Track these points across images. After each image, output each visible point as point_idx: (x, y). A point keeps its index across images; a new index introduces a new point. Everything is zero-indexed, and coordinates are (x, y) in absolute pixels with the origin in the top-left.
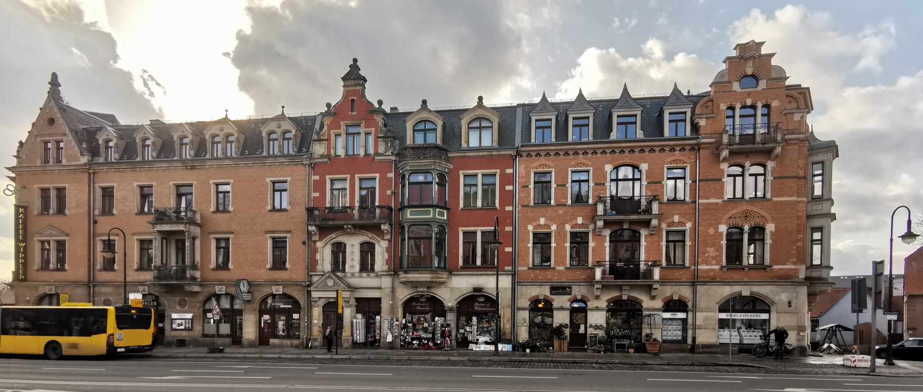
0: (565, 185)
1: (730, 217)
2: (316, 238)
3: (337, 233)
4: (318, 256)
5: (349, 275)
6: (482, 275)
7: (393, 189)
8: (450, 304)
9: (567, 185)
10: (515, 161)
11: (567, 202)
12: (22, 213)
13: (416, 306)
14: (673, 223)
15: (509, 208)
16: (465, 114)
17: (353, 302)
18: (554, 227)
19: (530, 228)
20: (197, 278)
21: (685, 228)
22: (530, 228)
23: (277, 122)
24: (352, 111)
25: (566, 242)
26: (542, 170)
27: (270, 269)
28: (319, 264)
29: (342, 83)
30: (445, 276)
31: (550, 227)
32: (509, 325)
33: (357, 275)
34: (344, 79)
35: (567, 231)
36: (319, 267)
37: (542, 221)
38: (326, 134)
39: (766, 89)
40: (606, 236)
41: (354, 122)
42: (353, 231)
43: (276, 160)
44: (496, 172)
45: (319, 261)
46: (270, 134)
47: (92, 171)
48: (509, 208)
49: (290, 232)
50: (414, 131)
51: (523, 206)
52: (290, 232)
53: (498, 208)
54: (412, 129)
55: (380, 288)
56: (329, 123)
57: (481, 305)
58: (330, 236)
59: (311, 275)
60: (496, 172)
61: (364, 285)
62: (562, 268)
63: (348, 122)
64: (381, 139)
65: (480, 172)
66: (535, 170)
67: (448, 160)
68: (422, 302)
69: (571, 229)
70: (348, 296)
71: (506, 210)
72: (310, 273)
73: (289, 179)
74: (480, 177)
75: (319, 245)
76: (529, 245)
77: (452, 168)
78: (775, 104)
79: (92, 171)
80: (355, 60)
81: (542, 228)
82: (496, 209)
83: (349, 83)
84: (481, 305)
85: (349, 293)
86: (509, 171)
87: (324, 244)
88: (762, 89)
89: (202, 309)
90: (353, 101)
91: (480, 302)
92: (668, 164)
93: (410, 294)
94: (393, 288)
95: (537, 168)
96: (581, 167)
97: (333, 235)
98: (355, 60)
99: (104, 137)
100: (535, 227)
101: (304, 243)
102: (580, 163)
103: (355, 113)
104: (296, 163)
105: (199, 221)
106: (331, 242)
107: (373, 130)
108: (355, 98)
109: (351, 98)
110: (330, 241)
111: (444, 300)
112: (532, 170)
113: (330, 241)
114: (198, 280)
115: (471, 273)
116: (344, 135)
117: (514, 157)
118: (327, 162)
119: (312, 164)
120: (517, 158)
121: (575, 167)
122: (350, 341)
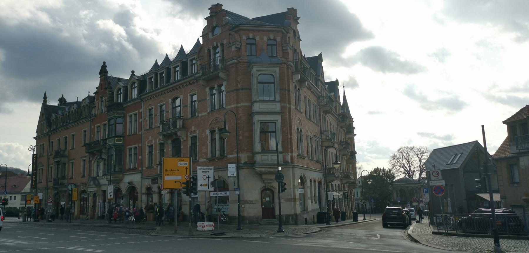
1: (211, 124)
6: (132, 174)
12: (35, 157)
14: (191, 132)
15: (140, 133)
18: (153, 142)
19: (147, 143)
20: (65, 184)
21: (196, 134)
22: (147, 143)
24: (102, 90)
30: (121, 176)
39: (221, 33)
40: (169, 144)
47: (49, 135)
70: (96, 190)
75: (93, 162)
78: (225, 42)
79: (49, 135)
85: (96, 188)
88: (220, 34)
89: (68, 199)
92: (189, 93)
99: (52, 119)
103: (102, 90)
105: (67, 155)
107: (106, 98)
108: (102, 83)
114: (65, 185)
115: (133, 172)
116: (100, 103)
118: (95, 118)
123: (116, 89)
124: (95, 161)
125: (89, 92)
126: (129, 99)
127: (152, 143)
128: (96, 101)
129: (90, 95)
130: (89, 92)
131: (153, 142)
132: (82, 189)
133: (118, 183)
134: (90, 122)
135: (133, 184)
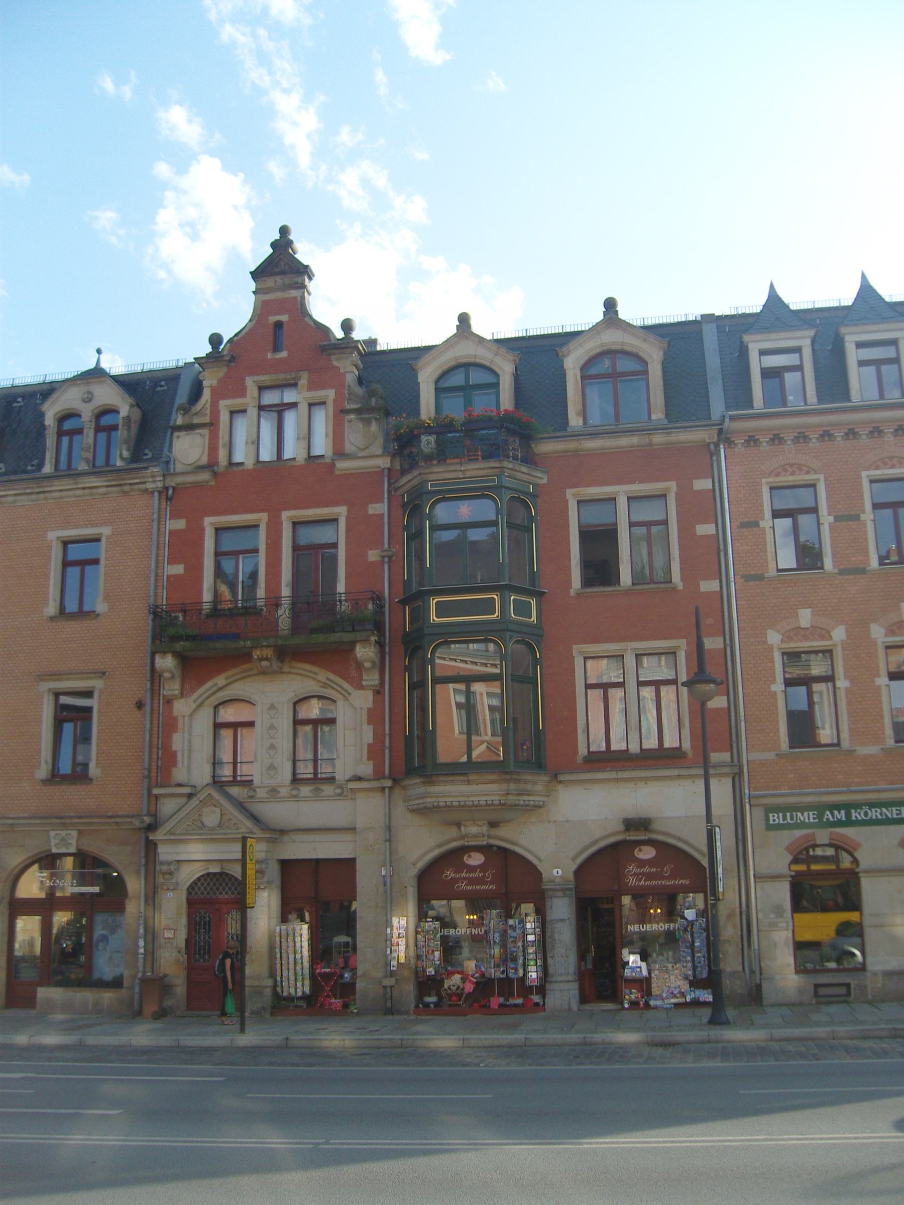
0: (857, 518)
2: (172, 688)
3: (230, 673)
4: (178, 742)
5: (261, 793)
6: (646, 780)
7: (386, 546)
8: (557, 872)
9: (863, 517)
10: (715, 458)
11: (867, 561)
13: (455, 881)
15: (709, 586)
16: (573, 345)
17: (274, 872)
18: (839, 634)
19: (774, 638)
23: (84, 388)
24: (276, 349)
25: (879, 676)
26: (791, 478)
27: (45, 782)
28: (180, 764)
29: (252, 285)
30: (539, 787)
31: (829, 632)
32: (734, 927)
33: (284, 792)
34: (256, 275)
35: (875, 643)
36: (179, 774)
37: (805, 618)
38: (208, 412)
41: (282, 376)
42: (276, 665)
43: (76, 483)
44: (668, 489)
45: (179, 755)
46: (63, 418)
48: (709, 586)
49: (104, 673)
50: (439, 391)
51: (748, 578)
52: (104, 673)
53: (680, 586)
54: (432, 387)
55: (352, 829)
56: (215, 383)
57: (646, 869)
58: (208, 685)
59: (157, 797)
60: (668, 489)
61: (302, 823)
62: (872, 750)
63: (265, 379)
64: (352, 416)
65: (621, 492)
66: (771, 480)
67: (529, 459)
68: (472, 869)
69: (886, 636)
71: (702, 590)
72: (155, 791)
73: (106, 531)
74: (622, 503)
75: (181, 708)
76: (773, 688)
77: (545, 481)
80: (284, 231)
81: (805, 638)
82: (674, 589)
83: (270, 282)
84: (646, 869)
86: (702, 484)
87: (194, 706)
90: (279, 325)
91: (642, 863)
93: (439, 846)
94: (389, 828)
95: (778, 475)
96: (893, 466)
97: (220, 680)
98: (284, 231)
100: (787, 636)
101: (140, 705)
102: (891, 458)
103: (284, 354)
104: (126, 488)
106: (213, 698)
108: (284, 318)
109: (273, 319)
110: (208, 698)
111: (541, 861)
112: (764, 481)
113: (208, 698)
115: (613, 775)
117: (712, 447)
119: (167, 489)
120: (722, 451)
121: (877, 468)
122: (268, 992)
123: (435, 364)
124: (203, 702)
125: (99, 351)
126: (575, 421)
127: (825, 634)
128: (218, 394)
129: (104, 365)
130: (99, 351)
131: (839, 634)
132: (68, 845)
133: (493, 825)
134: (156, 494)
135: (653, 831)
